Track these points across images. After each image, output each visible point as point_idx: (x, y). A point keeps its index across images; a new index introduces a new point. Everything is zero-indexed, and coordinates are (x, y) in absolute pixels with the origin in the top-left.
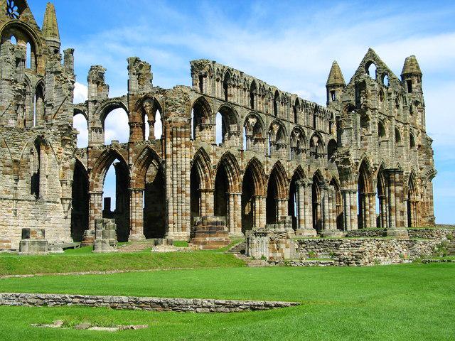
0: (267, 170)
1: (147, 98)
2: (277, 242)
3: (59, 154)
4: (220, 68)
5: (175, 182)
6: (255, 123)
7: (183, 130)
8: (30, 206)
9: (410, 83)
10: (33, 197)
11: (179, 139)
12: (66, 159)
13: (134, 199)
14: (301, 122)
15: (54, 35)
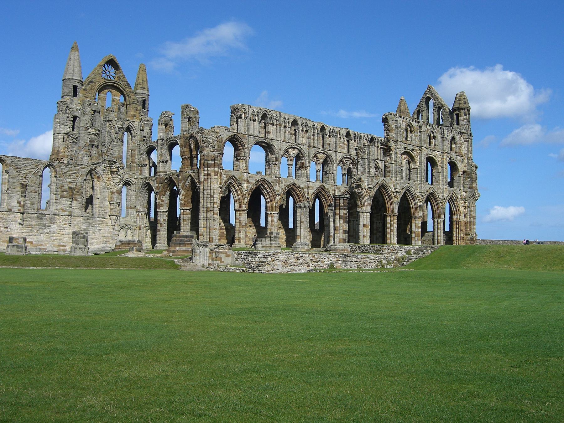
0: (308, 193)
1: (192, 137)
2: (216, 252)
3: (108, 182)
4: (256, 111)
6: (296, 154)
7: (213, 162)
12: (114, 186)
15: (143, 88)
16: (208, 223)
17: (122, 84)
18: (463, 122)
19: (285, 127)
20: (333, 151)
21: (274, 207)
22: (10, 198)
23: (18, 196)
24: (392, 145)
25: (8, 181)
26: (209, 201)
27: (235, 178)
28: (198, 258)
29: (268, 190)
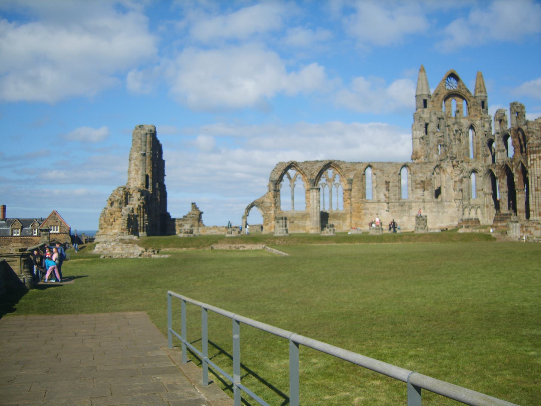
2: (526, 227)
5: (533, 184)
7: (537, 149)
11: (535, 155)
12: (456, 176)
15: (481, 92)
16: (537, 201)
17: (463, 91)
22: (378, 192)
26: (536, 182)
28: (511, 231)
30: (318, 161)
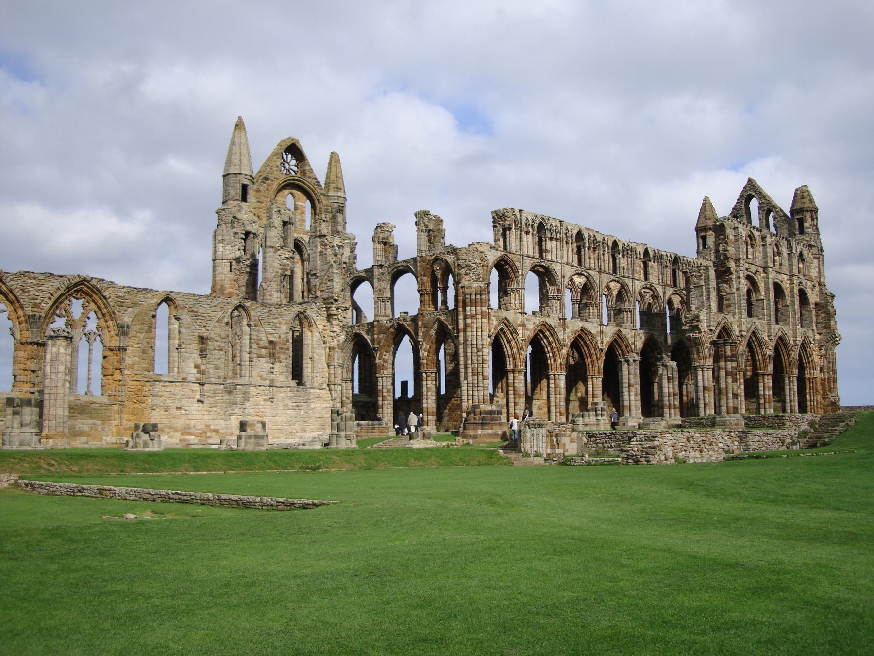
0: (602, 342)
1: (436, 259)
2: (557, 436)
4: (530, 218)
5: (469, 362)
6: (583, 283)
7: (479, 297)
8: (290, 394)
9: (801, 221)
10: (294, 383)
11: (474, 308)
12: (333, 338)
13: (424, 383)
14: (653, 279)
17: (309, 183)
18: (810, 231)
19: (567, 242)
20: (628, 277)
21: (559, 367)
23: (196, 358)
24: (732, 265)
25: (180, 332)
27: (508, 321)
28: (528, 445)
29: (551, 339)
30: (52, 275)
